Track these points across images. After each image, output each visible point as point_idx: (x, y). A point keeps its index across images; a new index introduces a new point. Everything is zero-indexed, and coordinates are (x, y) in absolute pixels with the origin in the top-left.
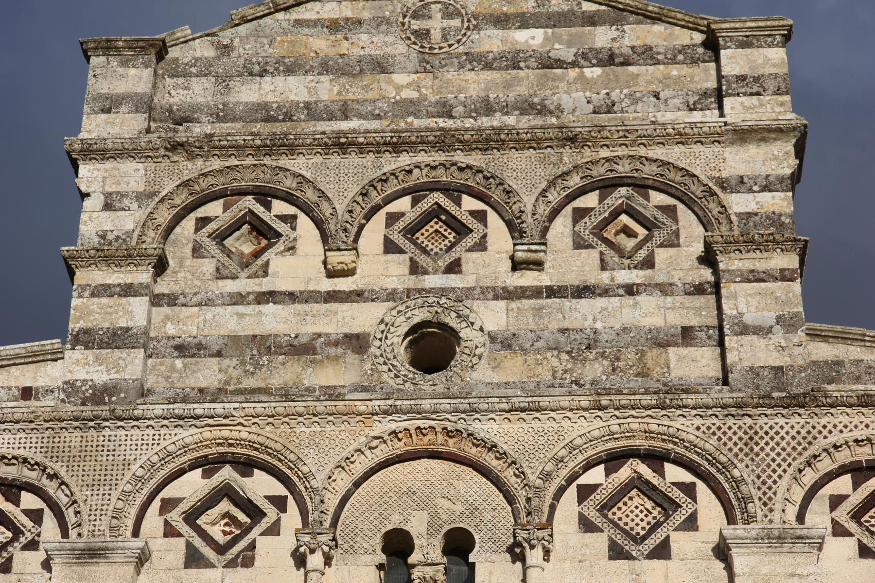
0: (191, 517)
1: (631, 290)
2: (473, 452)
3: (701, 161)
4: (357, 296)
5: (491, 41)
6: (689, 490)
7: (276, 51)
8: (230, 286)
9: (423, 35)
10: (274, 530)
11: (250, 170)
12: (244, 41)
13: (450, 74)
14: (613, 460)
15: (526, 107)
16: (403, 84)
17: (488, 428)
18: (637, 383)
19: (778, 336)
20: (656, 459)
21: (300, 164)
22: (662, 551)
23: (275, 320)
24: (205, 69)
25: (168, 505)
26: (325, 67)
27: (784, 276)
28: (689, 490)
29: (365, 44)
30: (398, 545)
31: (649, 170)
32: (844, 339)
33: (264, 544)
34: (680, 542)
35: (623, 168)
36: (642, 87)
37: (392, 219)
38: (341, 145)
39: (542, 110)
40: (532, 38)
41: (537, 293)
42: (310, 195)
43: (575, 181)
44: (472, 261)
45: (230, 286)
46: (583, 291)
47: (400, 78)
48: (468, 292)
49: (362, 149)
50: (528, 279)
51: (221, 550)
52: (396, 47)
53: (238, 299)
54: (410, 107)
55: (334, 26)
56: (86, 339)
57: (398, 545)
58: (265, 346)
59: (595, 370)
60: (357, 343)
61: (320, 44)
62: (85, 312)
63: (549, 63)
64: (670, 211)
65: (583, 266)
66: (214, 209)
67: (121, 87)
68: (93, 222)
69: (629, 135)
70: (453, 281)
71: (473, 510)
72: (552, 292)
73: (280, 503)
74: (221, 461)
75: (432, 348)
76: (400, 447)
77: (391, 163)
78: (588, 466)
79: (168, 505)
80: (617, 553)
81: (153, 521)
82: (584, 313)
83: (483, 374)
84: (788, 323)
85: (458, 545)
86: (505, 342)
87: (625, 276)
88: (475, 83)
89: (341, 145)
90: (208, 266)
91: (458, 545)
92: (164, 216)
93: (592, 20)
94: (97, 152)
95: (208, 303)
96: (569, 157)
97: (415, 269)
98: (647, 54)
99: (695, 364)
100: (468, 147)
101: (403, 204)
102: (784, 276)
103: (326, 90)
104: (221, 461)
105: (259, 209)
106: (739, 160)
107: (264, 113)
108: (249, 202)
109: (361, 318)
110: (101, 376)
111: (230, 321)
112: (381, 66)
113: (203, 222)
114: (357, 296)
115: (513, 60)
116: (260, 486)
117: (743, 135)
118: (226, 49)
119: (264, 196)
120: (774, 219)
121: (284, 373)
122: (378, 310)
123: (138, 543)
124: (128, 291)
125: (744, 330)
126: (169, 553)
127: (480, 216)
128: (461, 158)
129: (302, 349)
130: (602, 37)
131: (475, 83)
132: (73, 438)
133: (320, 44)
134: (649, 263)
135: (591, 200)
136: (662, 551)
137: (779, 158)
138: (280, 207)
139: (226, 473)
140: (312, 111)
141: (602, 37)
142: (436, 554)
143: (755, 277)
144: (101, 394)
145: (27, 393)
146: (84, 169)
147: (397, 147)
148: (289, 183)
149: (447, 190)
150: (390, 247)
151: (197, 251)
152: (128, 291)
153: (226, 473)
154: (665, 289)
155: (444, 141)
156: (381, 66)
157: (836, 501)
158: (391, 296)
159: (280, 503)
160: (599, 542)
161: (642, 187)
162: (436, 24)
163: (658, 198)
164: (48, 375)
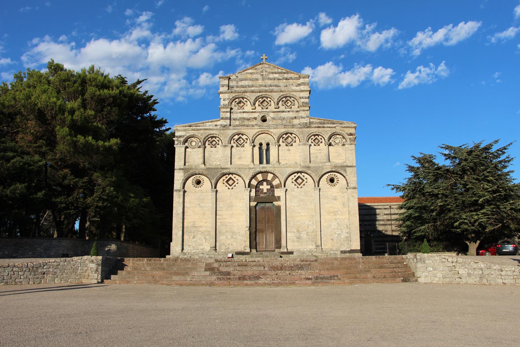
0: (236, 141)
1: (289, 112)
2: (270, 133)
3: (298, 95)
4: (255, 112)
5: (271, 76)
7: (244, 77)
8: (240, 111)
9: (262, 75)
10: (246, 143)
11: (241, 95)
13: (266, 81)
14: (286, 134)
15: (276, 86)
16: (260, 82)
17: (271, 130)
18: (289, 124)
19: (306, 119)
20: (291, 134)
21: (247, 94)
22: (292, 145)
23: (245, 115)
24: (235, 80)
25: (234, 139)
26: (250, 80)
27: (307, 110)
28: (295, 137)
29: (255, 76)
30: (261, 144)
31: (291, 95)
32: (314, 119)
33: (245, 144)
34: (294, 144)
35: (288, 95)
36: (291, 83)
37: (259, 101)
38: (253, 92)
39: (278, 86)
40: (276, 76)
41: (277, 112)
42: (249, 98)
44: (269, 107)
45: (240, 111)
46: (283, 112)
47: (260, 81)
49: (255, 92)
50: (277, 110)
51: (240, 145)
52: (259, 76)
53: (241, 112)
54: (261, 86)
55: (251, 73)
56: (222, 118)
57: (261, 144)
58: (244, 119)
59: (284, 122)
60: (255, 118)
61: (249, 76)
62: (222, 115)
63: (279, 79)
64: (294, 101)
65: (282, 108)
66: (237, 100)
67: (224, 83)
68: (222, 102)
69: (289, 91)
70: (267, 110)
71: (270, 140)
72: (279, 112)
73: (247, 139)
74: (240, 134)
75: (264, 120)
76: (261, 132)
77: (259, 94)
78: (283, 135)
79: (234, 139)
80: (287, 145)
81: (232, 142)
82: (283, 115)
83: (271, 123)
84: (308, 117)
85: (268, 144)
86: (273, 119)
88: (269, 82)
89: (253, 92)
90: (236, 108)
91: (268, 144)
92: (231, 101)
93: (284, 73)
94: (221, 93)
95: (237, 113)
96: (282, 94)
97: (262, 108)
98: (291, 78)
99: (296, 122)
100: (269, 92)
101: (261, 99)
102: (307, 110)
103: (250, 83)
104: (240, 134)
105: (242, 100)
106: (302, 94)
107: (242, 87)
108: (241, 99)
109: (255, 115)
110: (225, 124)
111: (240, 116)
112: (257, 80)
113: (236, 102)
114: (255, 112)
115: (274, 79)
117: (302, 91)
118: (237, 77)
119: (243, 98)
120: (306, 103)
121: (246, 123)
122: (258, 114)
123: (231, 145)
124: (227, 112)
125: (302, 118)
126: (235, 145)
127: (270, 101)
128: (268, 94)
129: (249, 119)
131: (269, 82)
132: (222, 131)
133: (249, 76)
134: (291, 108)
135: (284, 99)
136: (292, 145)
137: (307, 94)
138: (245, 100)
139: (240, 135)
140: (249, 86)
142: (266, 146)
143: (304, 111)
144: (225, 126)
145: (216, 125)
146: (221, 95)
147: (260, 92)
148: (246, 97)
149: (266, 97)
150: (259, 105)
151: (235, 106)
152: (227, 112)
153: (240, 135)
154: (293, 111)
156: (257, 80)
157: (312, 139)
158: (259, 112)
159: (247, 139)
160: (284, 144)
161: (290, 97)
162: (264, 73)
163: (292, 99)
164: (219, 123)
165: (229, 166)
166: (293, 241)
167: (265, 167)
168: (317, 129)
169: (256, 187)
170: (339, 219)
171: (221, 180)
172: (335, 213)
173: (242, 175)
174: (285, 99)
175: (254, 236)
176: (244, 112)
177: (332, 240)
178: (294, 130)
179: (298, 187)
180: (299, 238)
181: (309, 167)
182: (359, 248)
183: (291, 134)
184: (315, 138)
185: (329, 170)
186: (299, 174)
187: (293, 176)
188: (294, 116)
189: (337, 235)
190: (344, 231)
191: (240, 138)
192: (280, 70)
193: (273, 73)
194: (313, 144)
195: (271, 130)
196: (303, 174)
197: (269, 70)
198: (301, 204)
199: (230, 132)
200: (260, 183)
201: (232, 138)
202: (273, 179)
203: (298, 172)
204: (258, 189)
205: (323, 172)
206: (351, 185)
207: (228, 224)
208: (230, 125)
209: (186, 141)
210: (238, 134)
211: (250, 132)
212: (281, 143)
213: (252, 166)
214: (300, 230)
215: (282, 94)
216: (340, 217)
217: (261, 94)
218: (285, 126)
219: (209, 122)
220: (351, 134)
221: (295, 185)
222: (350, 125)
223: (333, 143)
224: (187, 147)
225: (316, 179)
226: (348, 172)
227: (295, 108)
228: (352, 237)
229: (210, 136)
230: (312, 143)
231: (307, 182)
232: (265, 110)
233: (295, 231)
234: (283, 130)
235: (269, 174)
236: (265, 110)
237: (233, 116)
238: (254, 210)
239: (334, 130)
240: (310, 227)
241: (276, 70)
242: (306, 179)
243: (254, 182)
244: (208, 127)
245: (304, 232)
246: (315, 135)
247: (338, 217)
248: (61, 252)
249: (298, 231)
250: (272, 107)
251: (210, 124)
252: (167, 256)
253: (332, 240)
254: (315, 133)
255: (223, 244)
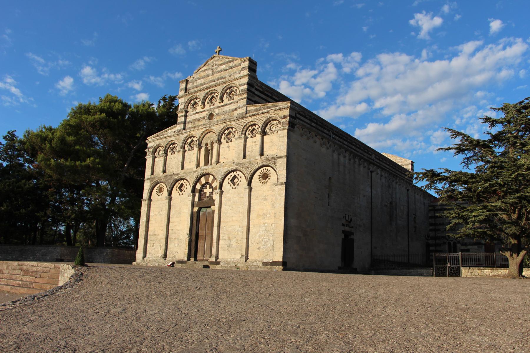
1: (231, 104)
5: (219, 69)
6: (235, 131)
8: (193, 112)
12: (196, 76)
14: (228, 129)
16: (210, 78)
17: (213, 128)
21: (198, 94)
22: (231, 141)
24: (192, 81)
29: (207, 73)
31: (233, 85)
35: (231, 85)
40: (223, 67)
43: (226, 88)
45: (193, 112)
46: (226, 105)
47: (210, 77)
48: (215, 108)
50: (222, 104)
53: (194, 114)
54: (210, 81)
55: (204, 71)
57: (207, 144)
60: (204, 118)
63: (225, 70)
70: (214, 106)
76: (206, 132)
78: (225, 131)
82: (226, 109)
86: (218, 115)
87: (231, 102)
88: (217, 76)
89: (201, 90)
92: (186, 105)
93: (230, 62)
96: (225, 85)
97: (210, 106)
98: (236, 66)
99: (236, 114)
107: (197, 86)
112: (208, 76)
116: (195, 139)
122: (206, 113)
124: (182, 116)
129: (199, 120)
130: (231, 64)
131: (217, 76)
133: (203, 74)
135: (228, 91)
141: (231, 64)
143: (242, 99)
154: (234, 103)
155: (211, 87)
156: (208, 76)
161: (234, 87)
165: (179, 171)
166: (224, 250)
167: (208, 169)
168: (252, 118)
169: (201, 191)
170: (267, 223)
171: (175, 186)
172: (264, 216)
173: (189, 180)
174: (229, 91)
175: (193, 244)
176: (196, 113)
177: (259, 248)
178: (233, 124)
179: (232, 188)
180: (229, 246)
181: (241, 164)
182: (281, 260)
183: (232, 128)
184: (248, 130)
185: (260, 165)
186: (235, 173)
187: (229, 176)
188: (235, 107)
189: (263, 243)
190: (271, 238)
191: (192, 141)
192: (227, 60)
193: (221, 65)
194: (249, 136)
195: (213, 128)
196: (238, 172)
197: (218, 63)
198: (234, 206)
199: (183, 137)
200: (204, 186)
201: (185, 142)
202: (213, 181)
203: (233, 171)
204: (202, 193)
205: (255, 168)
206: (280, 181)
207: (177, 232)
208: (184, 129)
209: (155, 151)
210: (190, 137)
211: (197, 133)
212: (222, 140)
213: (195, 169)
214: (231, 237)
215: (225, 85)
216: (268, 221)
217: (208, 90)
218: (224, 121)
219: (170, 129)
220: (285, 117)
221: (231, 186)
222: (283, 106)
223: (268, 132)
224: (156, 157)
225: (248, 177)
226: (278, 165)
227: (236, 98)
228: (275, 246)
229: (170, 143)
230: (249, 135)
231: (240, 181)
232: (212, 107)
233: (226, 238)
234: (223, 126)
235: (211, 176)
236: (212, 107)
237: (188, 119)
238: (195, 216)
239: (268, 116)
240: (239, 233)
241: (224, 61)
242: (241, 177)
243: (198, 186)
244: (169, 135)
245: (234, 240)
246: (252, 125)
247: (266, 221)
248: (55, 257)
249: (229, 238)
250: (217, 104)
251: (171, 130)
252: (134, 263)
253: (259, 248)
254: (252, 123)
255: (172, 252)
